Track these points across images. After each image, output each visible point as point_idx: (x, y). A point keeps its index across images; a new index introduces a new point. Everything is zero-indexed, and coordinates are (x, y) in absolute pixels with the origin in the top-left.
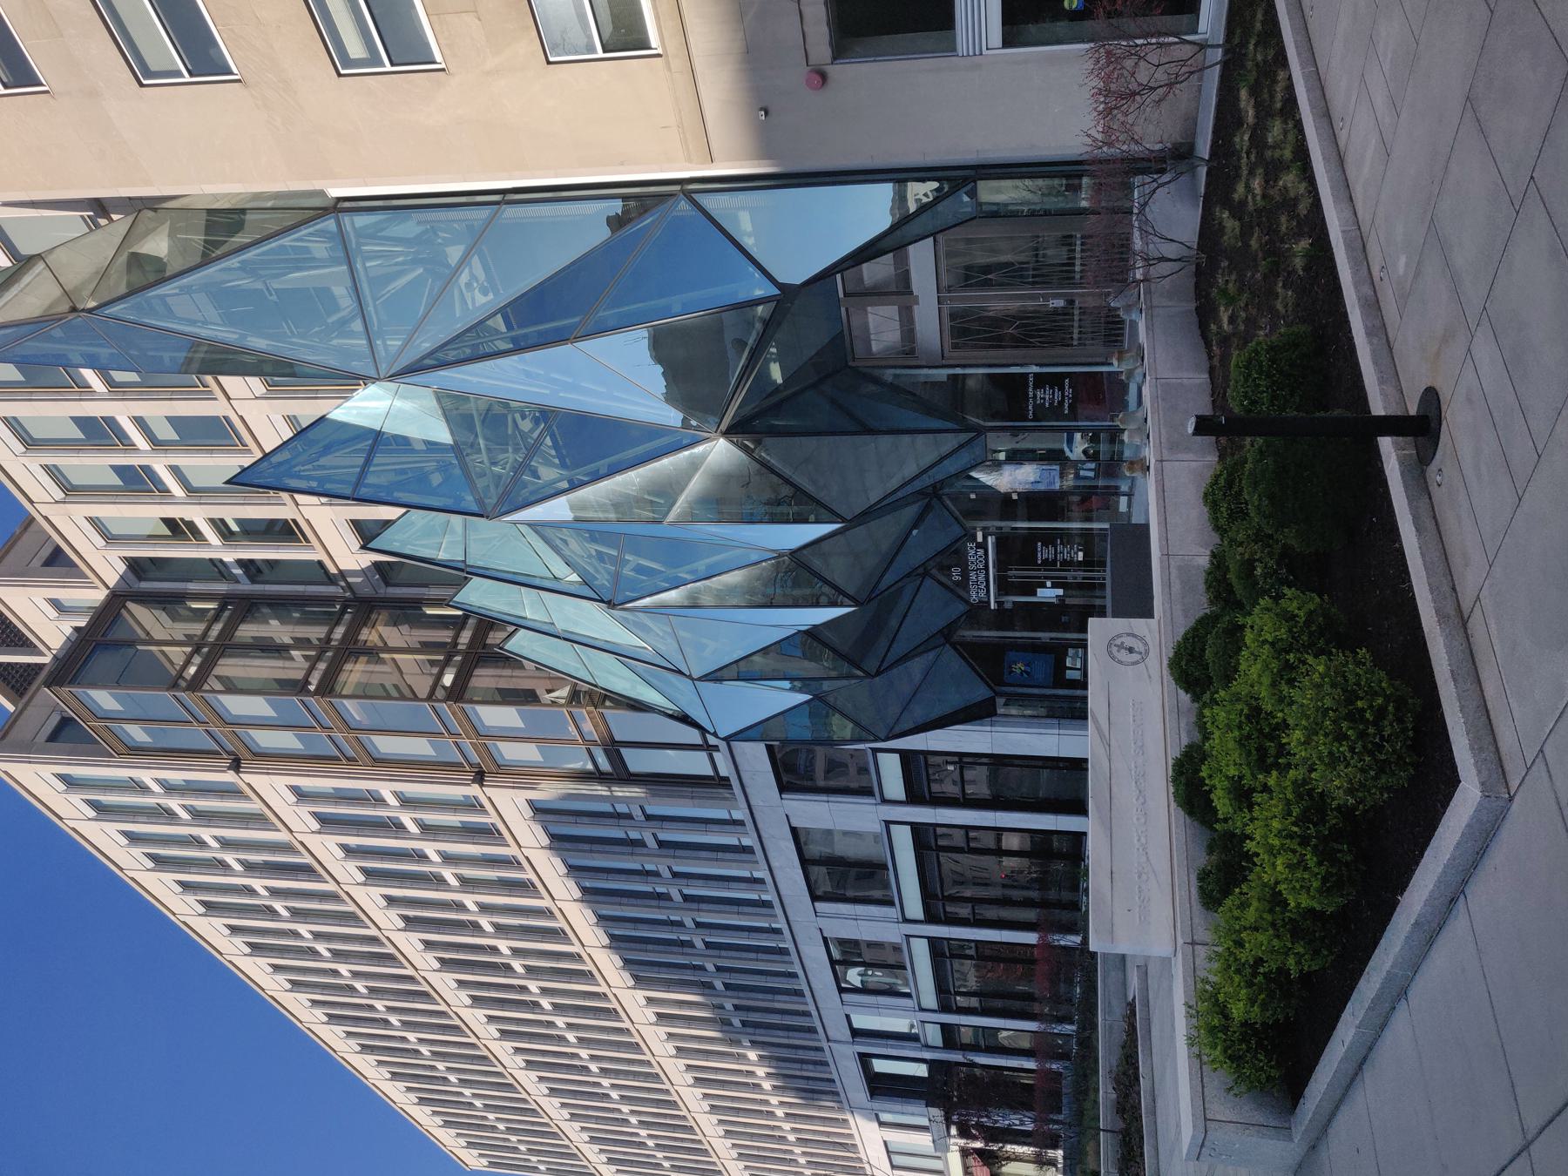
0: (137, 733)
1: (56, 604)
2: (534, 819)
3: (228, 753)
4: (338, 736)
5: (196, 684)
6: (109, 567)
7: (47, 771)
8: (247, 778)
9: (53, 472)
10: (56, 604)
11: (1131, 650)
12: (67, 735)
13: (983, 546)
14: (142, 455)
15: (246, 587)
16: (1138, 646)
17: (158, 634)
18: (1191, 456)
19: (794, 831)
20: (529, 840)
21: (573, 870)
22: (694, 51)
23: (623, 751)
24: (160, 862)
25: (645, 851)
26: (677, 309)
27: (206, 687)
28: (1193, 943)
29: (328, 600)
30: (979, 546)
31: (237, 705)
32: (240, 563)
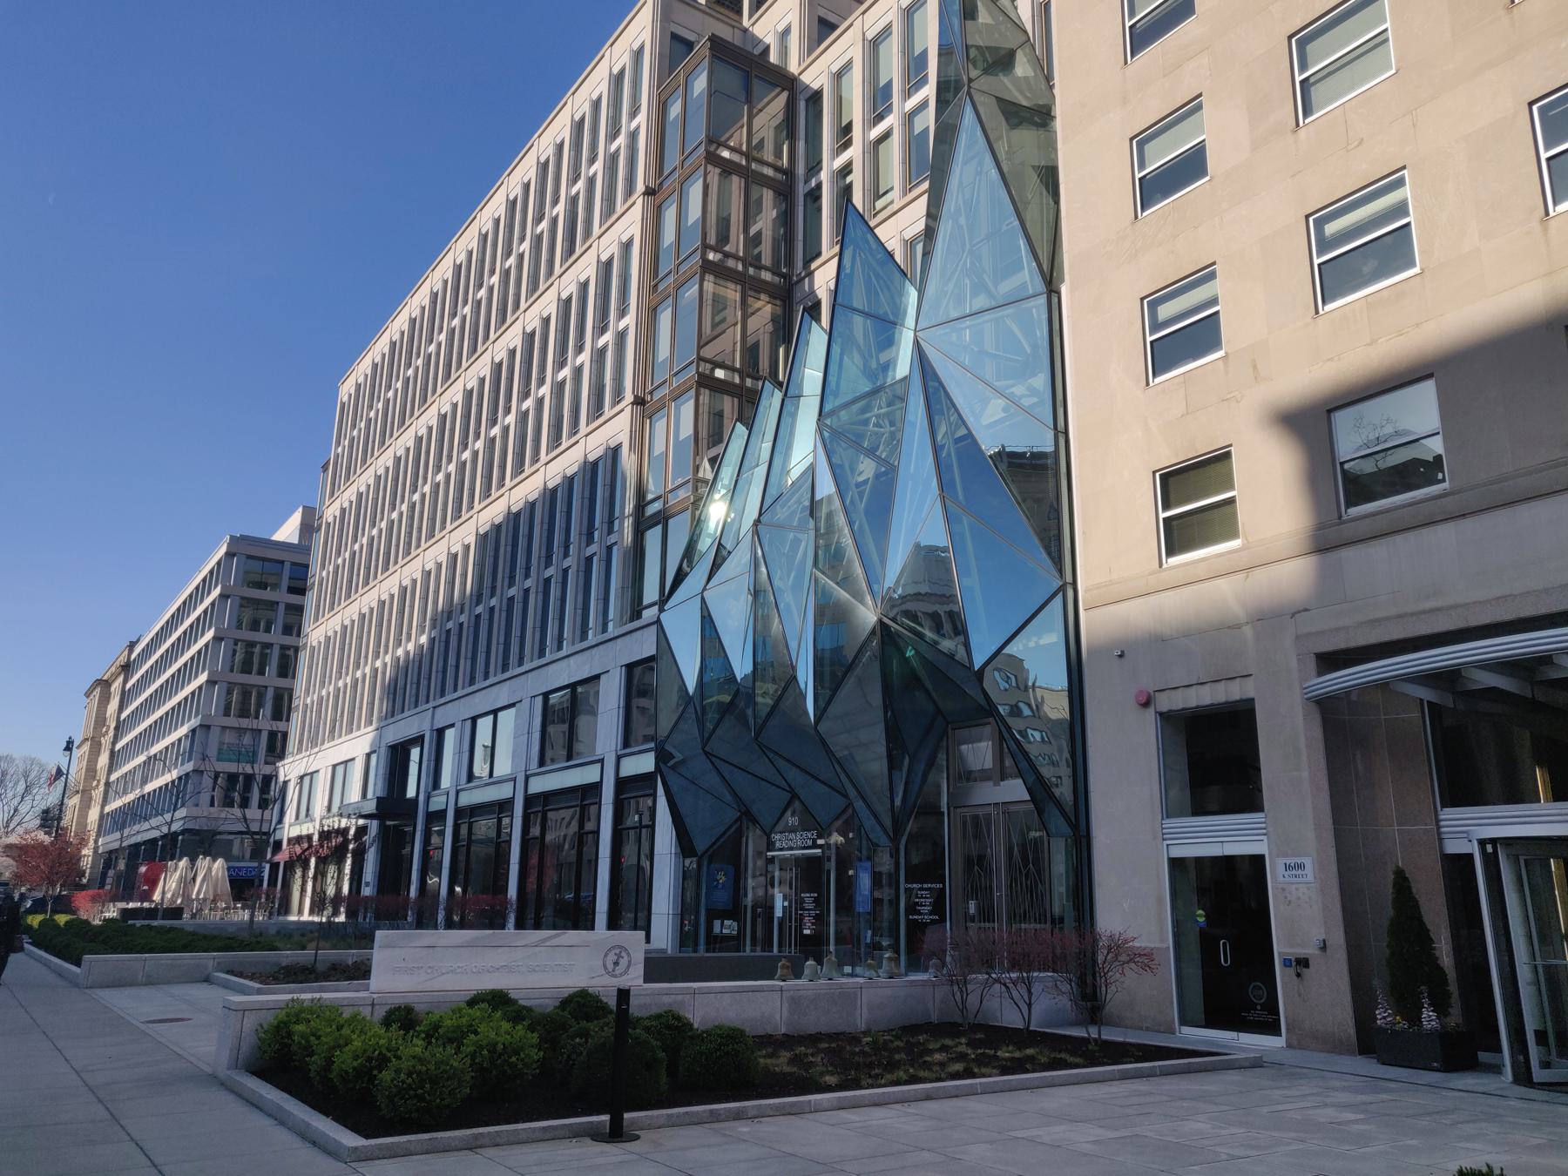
0: (675, 110)
1: (787, 31)
2: (608, 448)
3: (661, 184)
4: (671, 279)
5: (712, 159)
6: (815, 76)
7: (646, 36)
8: (640, 201)
9: (886, 31)
10: (787, 31)
11: (616, 963)
12: (675, 47)
13: (815, 846)
14: (901, 106)
15: (801, 190)
16: (619, 969)
17: (757, 122)
18: (785, 1014)
19: (597, 677)
20: (590, 444)
21: (569, 481)
22: (1163, 595)
23: (660, 527)
24: (578, 126)
25: (584, 544)
26: (966, 582)
27: (710, 167)
28: (373, 1005)
29: (790, 262)
30: (814, 841)
31: (695, 192)
32: (819, 186)
